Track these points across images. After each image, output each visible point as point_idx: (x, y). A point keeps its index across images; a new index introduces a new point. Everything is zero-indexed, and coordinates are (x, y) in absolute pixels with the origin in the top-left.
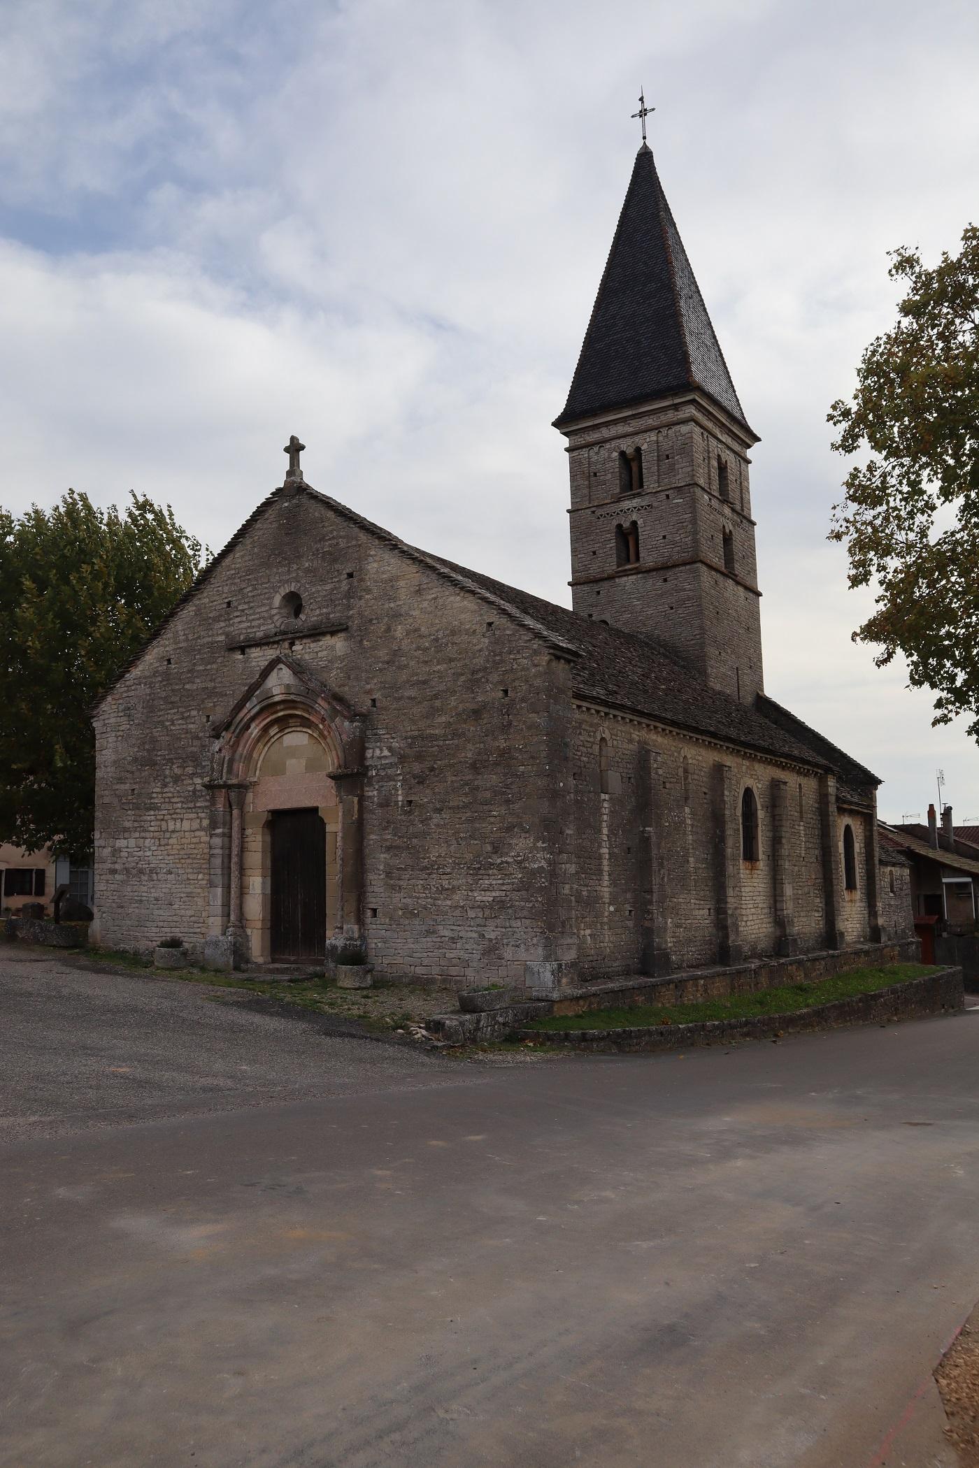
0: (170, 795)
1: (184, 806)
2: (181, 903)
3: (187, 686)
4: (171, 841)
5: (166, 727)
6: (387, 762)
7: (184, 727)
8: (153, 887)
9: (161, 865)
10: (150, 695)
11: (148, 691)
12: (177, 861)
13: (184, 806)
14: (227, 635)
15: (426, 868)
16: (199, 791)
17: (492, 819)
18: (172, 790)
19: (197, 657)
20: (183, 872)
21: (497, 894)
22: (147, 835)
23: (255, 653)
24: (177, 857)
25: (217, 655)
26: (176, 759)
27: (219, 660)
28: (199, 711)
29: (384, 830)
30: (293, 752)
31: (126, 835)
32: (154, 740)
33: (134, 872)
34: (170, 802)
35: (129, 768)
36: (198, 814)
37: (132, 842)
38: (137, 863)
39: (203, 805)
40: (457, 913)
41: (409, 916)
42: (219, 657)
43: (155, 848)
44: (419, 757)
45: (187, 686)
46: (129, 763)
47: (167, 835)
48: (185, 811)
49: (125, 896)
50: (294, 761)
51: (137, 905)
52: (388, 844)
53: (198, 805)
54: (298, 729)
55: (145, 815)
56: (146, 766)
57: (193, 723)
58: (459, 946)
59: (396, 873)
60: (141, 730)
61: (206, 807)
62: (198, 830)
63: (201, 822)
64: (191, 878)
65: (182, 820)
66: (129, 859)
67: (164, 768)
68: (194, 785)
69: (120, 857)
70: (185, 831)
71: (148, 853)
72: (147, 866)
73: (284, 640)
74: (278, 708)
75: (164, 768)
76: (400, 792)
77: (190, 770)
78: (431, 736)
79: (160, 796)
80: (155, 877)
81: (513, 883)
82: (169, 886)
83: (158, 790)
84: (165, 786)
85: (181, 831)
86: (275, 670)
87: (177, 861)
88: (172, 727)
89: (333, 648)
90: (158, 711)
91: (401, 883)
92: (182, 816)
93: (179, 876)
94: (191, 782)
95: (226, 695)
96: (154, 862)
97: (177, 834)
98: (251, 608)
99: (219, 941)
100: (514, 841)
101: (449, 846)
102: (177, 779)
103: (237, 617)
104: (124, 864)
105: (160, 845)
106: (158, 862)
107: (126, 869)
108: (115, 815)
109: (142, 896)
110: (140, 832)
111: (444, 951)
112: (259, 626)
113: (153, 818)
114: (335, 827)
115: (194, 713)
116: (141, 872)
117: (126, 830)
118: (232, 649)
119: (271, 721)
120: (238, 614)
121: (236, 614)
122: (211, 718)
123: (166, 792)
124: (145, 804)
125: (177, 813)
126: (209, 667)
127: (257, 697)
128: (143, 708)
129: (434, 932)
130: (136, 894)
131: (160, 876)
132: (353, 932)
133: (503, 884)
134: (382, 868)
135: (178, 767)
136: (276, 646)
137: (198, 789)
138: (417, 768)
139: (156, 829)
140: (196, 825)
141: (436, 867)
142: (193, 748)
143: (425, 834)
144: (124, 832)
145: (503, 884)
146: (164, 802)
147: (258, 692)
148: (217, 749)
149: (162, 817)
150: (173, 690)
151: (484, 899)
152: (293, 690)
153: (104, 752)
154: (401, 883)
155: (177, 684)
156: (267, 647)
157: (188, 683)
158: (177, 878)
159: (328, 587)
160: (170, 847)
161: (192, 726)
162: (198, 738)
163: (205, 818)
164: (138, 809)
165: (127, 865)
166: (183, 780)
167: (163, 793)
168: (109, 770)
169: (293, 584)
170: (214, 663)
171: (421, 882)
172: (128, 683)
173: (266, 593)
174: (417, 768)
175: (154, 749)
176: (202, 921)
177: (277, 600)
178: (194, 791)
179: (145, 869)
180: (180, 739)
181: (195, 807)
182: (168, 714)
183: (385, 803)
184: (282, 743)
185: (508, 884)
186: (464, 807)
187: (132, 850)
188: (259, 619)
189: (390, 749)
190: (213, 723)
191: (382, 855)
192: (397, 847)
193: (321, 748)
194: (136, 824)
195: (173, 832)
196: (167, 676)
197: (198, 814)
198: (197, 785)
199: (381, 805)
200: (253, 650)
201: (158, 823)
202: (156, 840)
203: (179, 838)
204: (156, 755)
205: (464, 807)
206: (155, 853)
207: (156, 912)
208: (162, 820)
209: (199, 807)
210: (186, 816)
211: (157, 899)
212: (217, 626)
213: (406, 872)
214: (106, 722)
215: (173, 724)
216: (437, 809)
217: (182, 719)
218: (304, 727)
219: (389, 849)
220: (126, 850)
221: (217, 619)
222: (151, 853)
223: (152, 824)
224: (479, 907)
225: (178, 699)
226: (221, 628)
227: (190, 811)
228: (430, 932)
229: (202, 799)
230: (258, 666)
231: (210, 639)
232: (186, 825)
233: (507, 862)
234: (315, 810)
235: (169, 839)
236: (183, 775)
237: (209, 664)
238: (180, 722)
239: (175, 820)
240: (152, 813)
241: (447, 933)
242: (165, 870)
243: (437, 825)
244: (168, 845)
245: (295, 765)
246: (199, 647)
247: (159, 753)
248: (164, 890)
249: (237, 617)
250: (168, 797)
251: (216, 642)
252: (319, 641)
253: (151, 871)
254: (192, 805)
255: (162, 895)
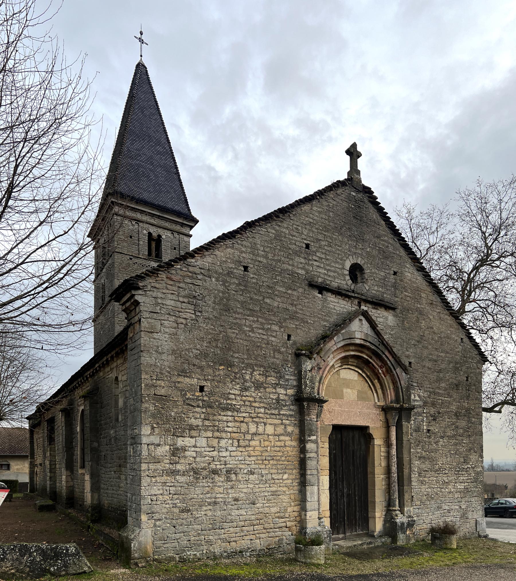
0: (251, 399)
1: (267, 411)
2: (265, 502)
3: (268, 301)
4: (253, 443)
5: (244, 332)
6: (418, 404)
7: (265, 337)
8: (232, 488)
9: (241, 466)
10: (223, 293)
11: (221, 288)
12: (261, 462)
13: (267, 411)
14: (307, 272)
15: (437, 470)
16: (282, 400)
17: (464, 444)
18: (253, 394)
19: (278, 278)
20: (267, 472)
21: (466, 484)
22: (224, 435)
23: (331, 298)
24: (259, 458)
25: (298, 285)
26: (256, 365)
27: (300, 290)
28: (281, 327)
29: (418, 446)
30: (347, 383)
31: (194, 433)
32: (228, 340)
33: (205, 473)
34: (251, 406)
35: (196, 362)
36: (282, 421)
37: (202, 442)
38: (210, 464)
39: (287, 413)
40: (451, 496)
41: (430, 499)
42: (300, 287)
43: (234, 449)
44: (433, 405)
45: (268, 301)
46: (196, 357)
47: (249, 437)
48: (268, 417)
49: (191, 499)
50: (349, 390)
51: (210, 507)
52: (419, 455)
53: (282, 413)
54: (352, 368)
55: (220, 415)
56: (221, 365)
57: (274, 337)
58: (451, 514)
59: (423, 473)
60: (212, 325)
61: (291, 416)
62: (282, 435)
63: (285, 428)
64: (275, 478)
65: (265, 424)
66: (198, 459)
67: (244, 372)
68: (277, 395)
69: (185, 457)
70: (268, 435)
71: (224, 454)
72: (223, 466)
73: (355, 298)
74: (351, 348)
75: (244, 372)
76: (425, 424)
77: (272, 380)
78: (439, 393)
79: (238, 398)
80: (233, 477)
81: (471, 479)
82: (251, 486)
83: (237, 392)
84: (246, 389)
85: (264, 434)
86: (357, 319)
87: (261, 462)
88: (250, 334)
89: (387, 318)
90: (235, 313)
91: (426, 479)
92: (265, 420)
93: (263, 476)
94: (274, 391)
95: (307, 322)
96: (232, 463)
97: (261, 437)
98: (327, 259)
99: (320, 532)
100: (471, 457)
101: (447, 458)
102: (258, 386)
103: (316, 261)
104: (190, 464)
105: (239, 446)
106: (238, 462)
107: (193, 469)
108: (175, 410)
109: (215, 498)
110: (213, 431)
111: (445, 517)
112: (334, 277)
113: (230, 418)
114: (378, 441)
115: (276, 328)
116: (215, 472)
117: (191, 428)
118: (312, 285)
119: (354, 355)
120: (317, 259)
121: (314, 258)
122: (292, 338)
123: (247, 396)
124: (221, 404)
125: (260, 417)
126: (290, 292)
127: (342, 334)
128: (214, 302)
129: (441, 508)
130: (208, 496)
131: (240, 477)
132: (410, 513)
133: (468, 479)
134: (416, 470)
135: (260, 374)
136: (347, 299)
137: (281, 398)
138: (432, 411)
139: (235, 430)
140: (280, 430)
141: (442, 470)
142: (275, 360)
143: (436, 451)
144: (190, 430)
145: (468, 479)
146: (244, 405)
147: (343, 331)
148: (309, 368)
149: (242, 419)
150: (251, 299)
151: (461, 487)
152: (369, 339)
153: (155, 335)
154: (426, 479)
155: (256, 294)
156: (340, 297)
157: (267, 298)
158: (261, 478)
159: (383, 274)
160: (251, 449)
161: (273, 339)
162: (280, 352)
163: (289, 425)
164: (211, 407)
165: (194, 465)
166: (265, 388)
167: (242, 396)
168: (164, 357)
169: (360, 259)
170: (295, 290)
171: (435, 479)
172: (191, 269)
173: (338, 254)
174: (432, 411)
175: (229, 349)
176: (288, 516)
177: (348, 265)
178: (278, 400)
179: (220, 469)
180: (262, 348)
181: (279, 414)
182: (246, 319)
183: (418, 430)
184: (339, 375)
185: (470, 479)
186: (452, 437)
187: (203, 449)
188: (335, 272)
189: (419, 396)
190: (295, 343)
191: (416, 462)
192: (424, 458)
193: (367, 385)
194: (207, 423)
195: (255, 434)
196: (244, 283)
197: (282, 421)
198: (281, 395)
199: (416, 431)
200: (329, 294)
201: (238, 424)
202: (235, 441)
203: (262, 440)
204: (232, 356)
205: (452, 437)
206: (233, 454)
207: (235, 513)
208: (242, 422)
209: (283, 415)
210: (269, 421)
211: (236, 500)
212: (297, 259)
213: (428, 473)
214: (160, 301)
215: (252, 331)
216: (442, 436)
217: (263, 329)
218: (356, 367)
219: (420, 458)
220: (193, 449)
221: (297, 253)
222: (228, 454)
223: (230, 424)
224: (459, 492)
225: (257, 308)
226: (301, 263)
227: (274, 417)
228: (439, 508)
229: (285, 408)
230: (335, 309)
231: (290, 268)
232: (270, 429)
233: (469, 468)
234: (367, 428)
235: (249, 441)
236: (266, 383)
237: (290, 289)
238: (260, 331)
239: (257, 423)
240: (230, 413)
241: (447, 508)
242: (245, 471)
243: (442, 446)
244: (249, 446)
245: (350, 394)
246: (279, 270)
247: (236, 355)
248: (245, 490)
249: (316, 261)
250: (249, 401)
251: (297, 274)
252: (377, 309)
253: (228, 472)
254: (276, 412)
255: (242, 495)
